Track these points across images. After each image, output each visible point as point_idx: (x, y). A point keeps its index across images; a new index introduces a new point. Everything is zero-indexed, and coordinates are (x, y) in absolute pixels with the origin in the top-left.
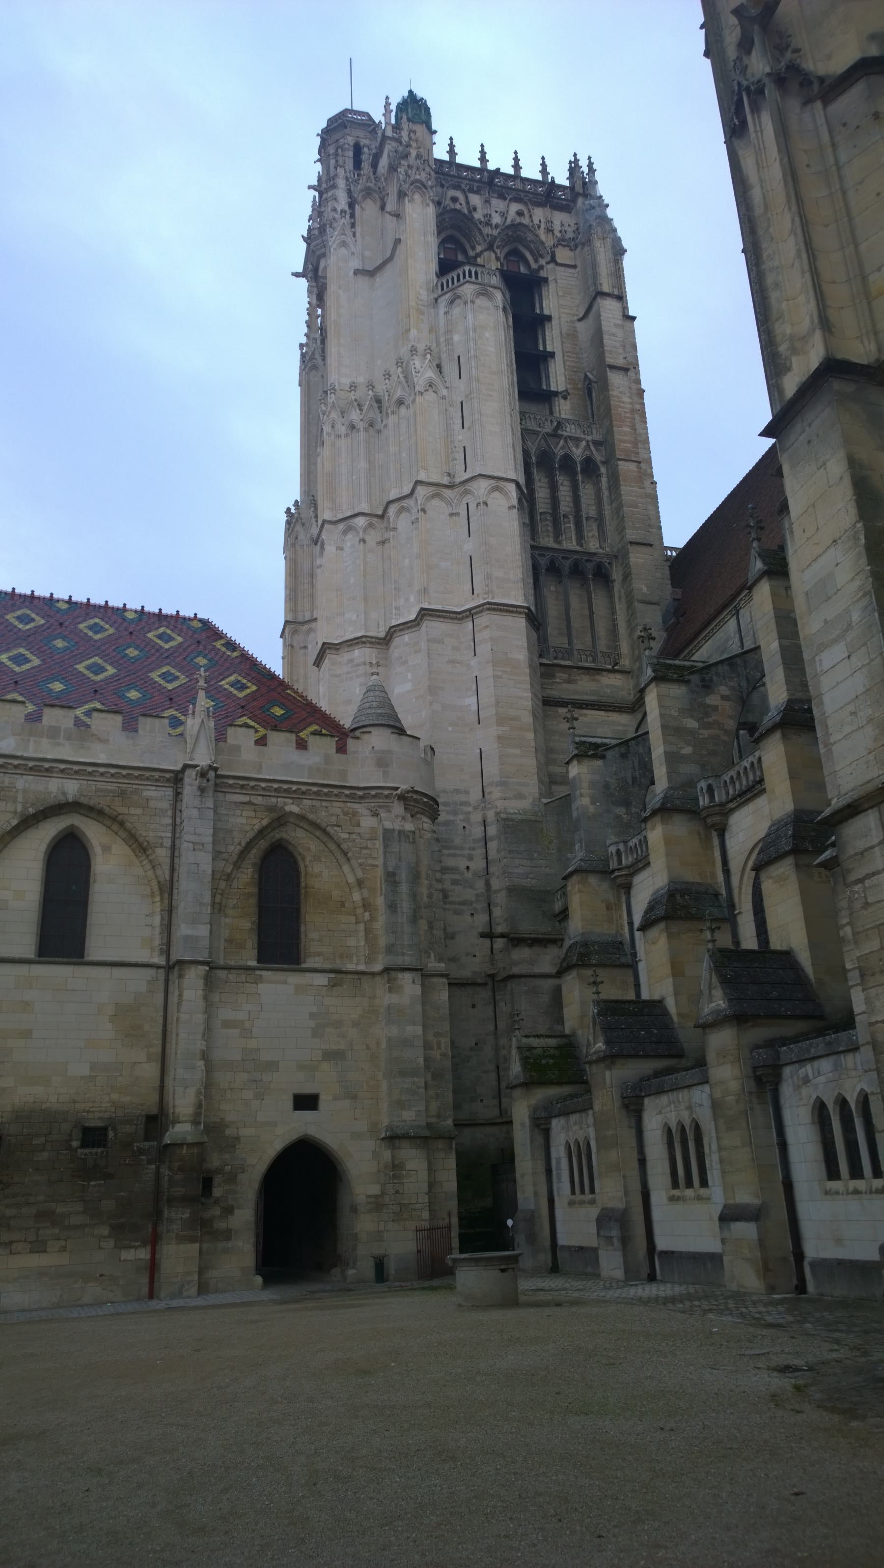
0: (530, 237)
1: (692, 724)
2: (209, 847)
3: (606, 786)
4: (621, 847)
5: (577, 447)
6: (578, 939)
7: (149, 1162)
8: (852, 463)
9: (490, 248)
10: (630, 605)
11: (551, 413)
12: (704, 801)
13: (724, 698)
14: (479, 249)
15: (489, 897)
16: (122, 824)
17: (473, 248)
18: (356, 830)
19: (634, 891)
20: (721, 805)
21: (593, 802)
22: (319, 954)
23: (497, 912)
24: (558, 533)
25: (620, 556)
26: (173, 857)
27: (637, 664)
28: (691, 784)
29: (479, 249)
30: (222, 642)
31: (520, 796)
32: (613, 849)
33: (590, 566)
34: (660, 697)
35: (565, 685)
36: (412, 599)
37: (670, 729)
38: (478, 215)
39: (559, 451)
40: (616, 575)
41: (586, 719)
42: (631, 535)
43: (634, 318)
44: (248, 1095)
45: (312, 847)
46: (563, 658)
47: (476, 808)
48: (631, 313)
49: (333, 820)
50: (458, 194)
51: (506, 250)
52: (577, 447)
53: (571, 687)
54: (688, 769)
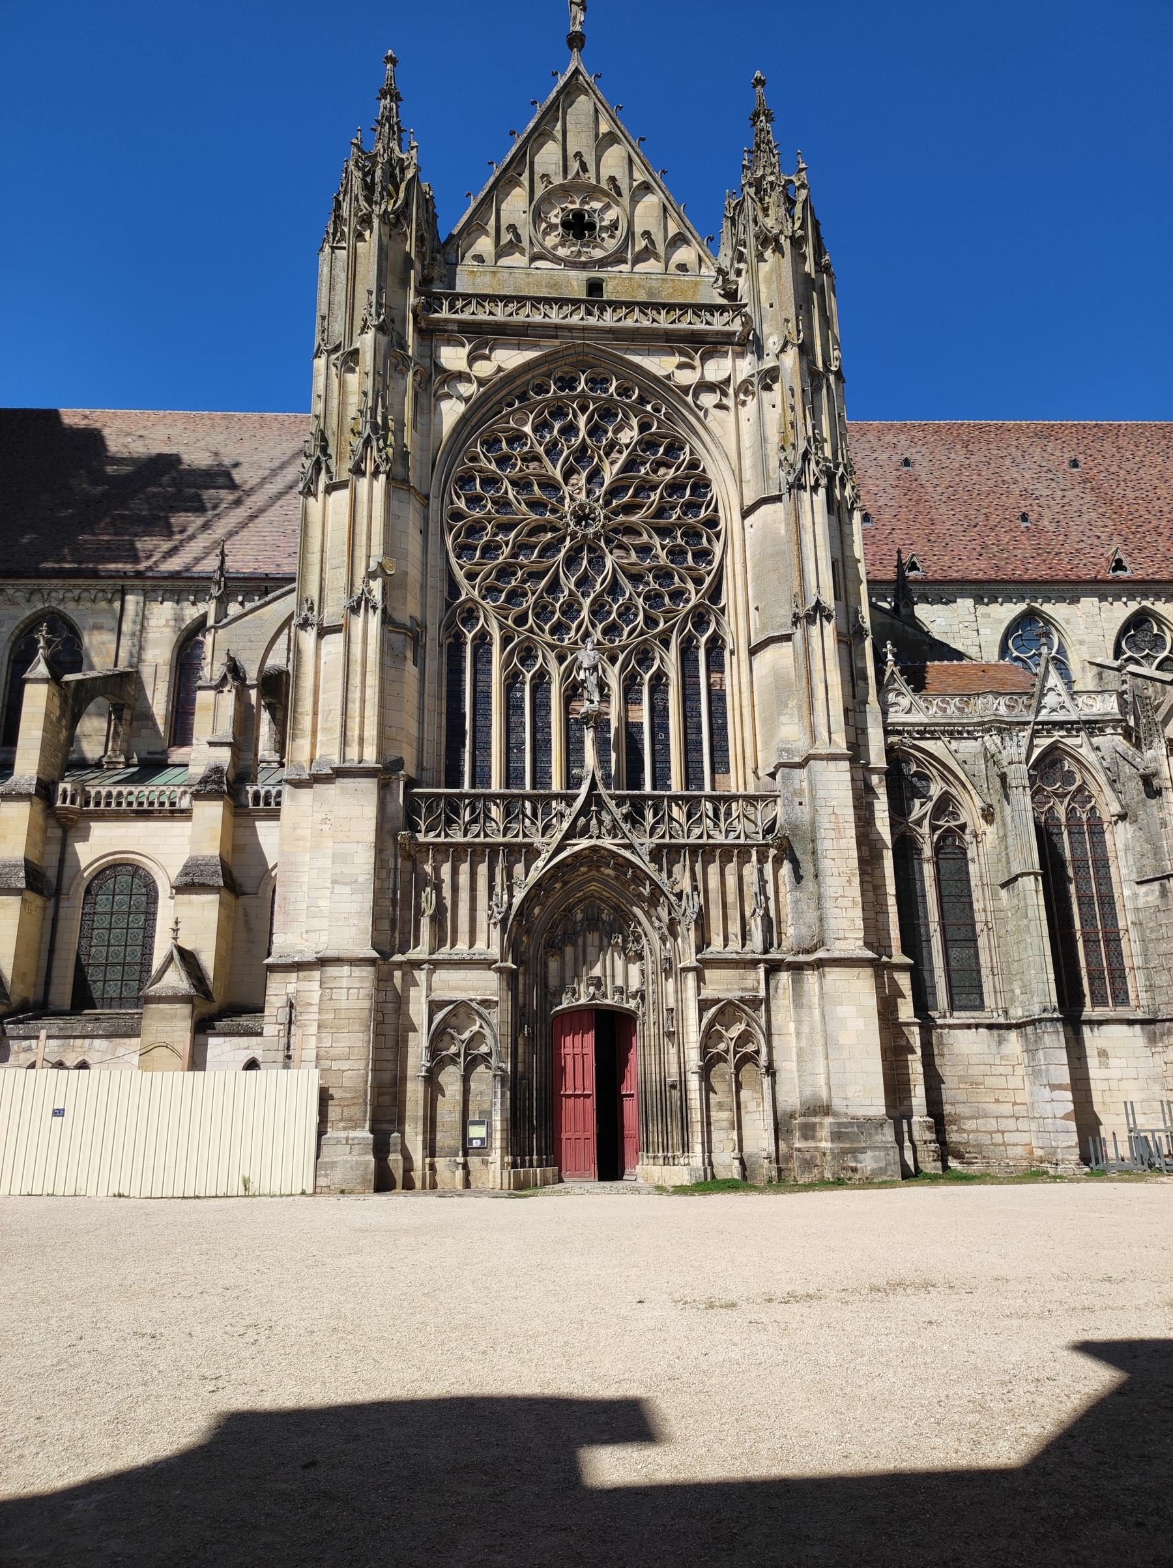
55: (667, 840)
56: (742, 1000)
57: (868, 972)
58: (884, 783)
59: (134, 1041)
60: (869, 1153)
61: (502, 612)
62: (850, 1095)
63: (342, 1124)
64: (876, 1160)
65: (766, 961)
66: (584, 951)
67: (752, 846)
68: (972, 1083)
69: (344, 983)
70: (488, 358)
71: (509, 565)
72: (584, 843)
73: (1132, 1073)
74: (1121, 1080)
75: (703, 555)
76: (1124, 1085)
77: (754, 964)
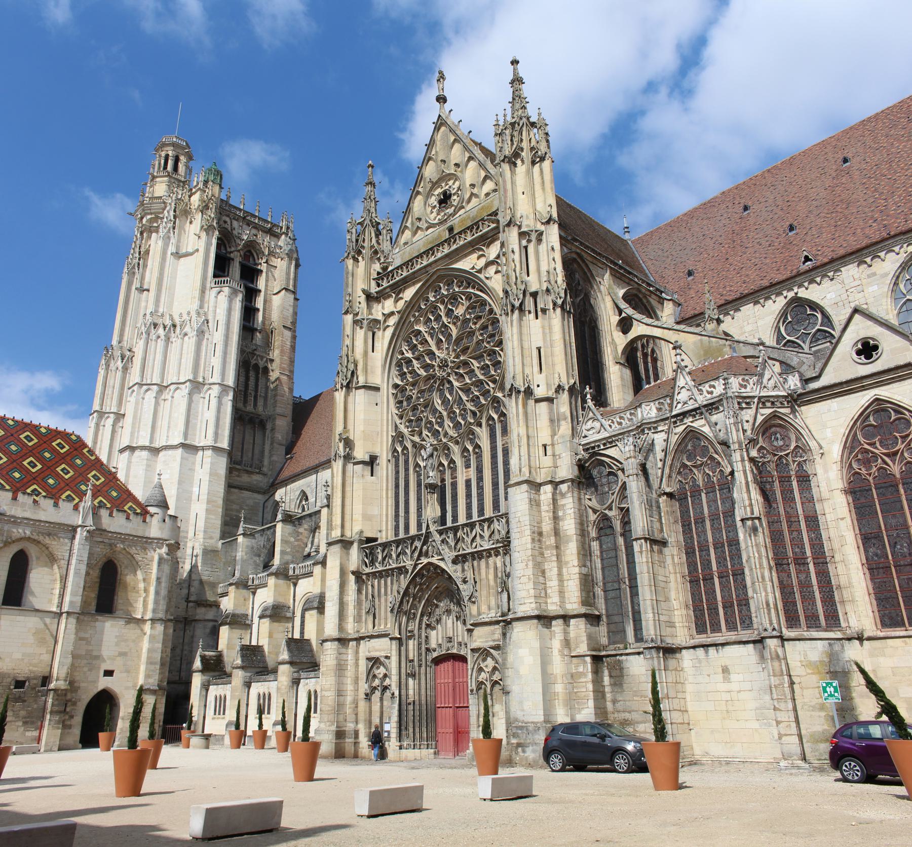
0: (258, 247)
1: (292, 539)
2: (86, 563)
3: (252, 548)
4: (255, 576)
5: (262, 360)
6: (231, 612)
7: (42, 696)
8: (341, 564)
9: (239, 251)
10: (272, 444)
11: (252, 339)
12: (291, 573)
13: (305, 529)
14: (233, 249)
15: (190, 582)
16: (47, 548)
17: (230, 247)
18: (146, 556)
19: (256, 594)
20: (297, 576)
21: (246, 555)
22: (122, 610)
23: (192, 589)
24: (245, 402)
25: (272, 418)
26: (68, 565)
27: (270, 473)
28: (287, 563)
29: (233, 249)
30: (86, 450)
31: (211, 538)
32: (251, 576)
33: (257, 420)
34: (282, 528)
35: (236, 478)
36: (176, 433)
37: (284, 541)
38: (235, 232)
39: (253, 362)
40: (269, 426)
41: (243, 495)
42: (279, 410)
43: (298, 300)
44: (86, 669)
45: (125, 562)
46: (237, 464)
47: (190, 540)
48: (298, 297)
49: (136, 552)
50: (228, 219)
51: (245, 250)
52: (262, 360)
53: (238, 479)
54: (289, 557)
55: (461, 552)
56: (492, 648)
57: (584, 619)
58: (571, 489)
59: (229, 685)
60: (531, 748)
61: (412, 433)
62: (525, 708)
63: (328, 724)
64: (534, 751)
65: (503, 621)
66: (446, 623)
67: (500, 547)
68: (641, 696)
69: (329, 652)
70: (402, 298)
71: (415, 405)
72: (424, 561)
73: (748, 686)
74: (739, 692)
75: (497, 364)
76: (742, 696)
77: (497, 622)
